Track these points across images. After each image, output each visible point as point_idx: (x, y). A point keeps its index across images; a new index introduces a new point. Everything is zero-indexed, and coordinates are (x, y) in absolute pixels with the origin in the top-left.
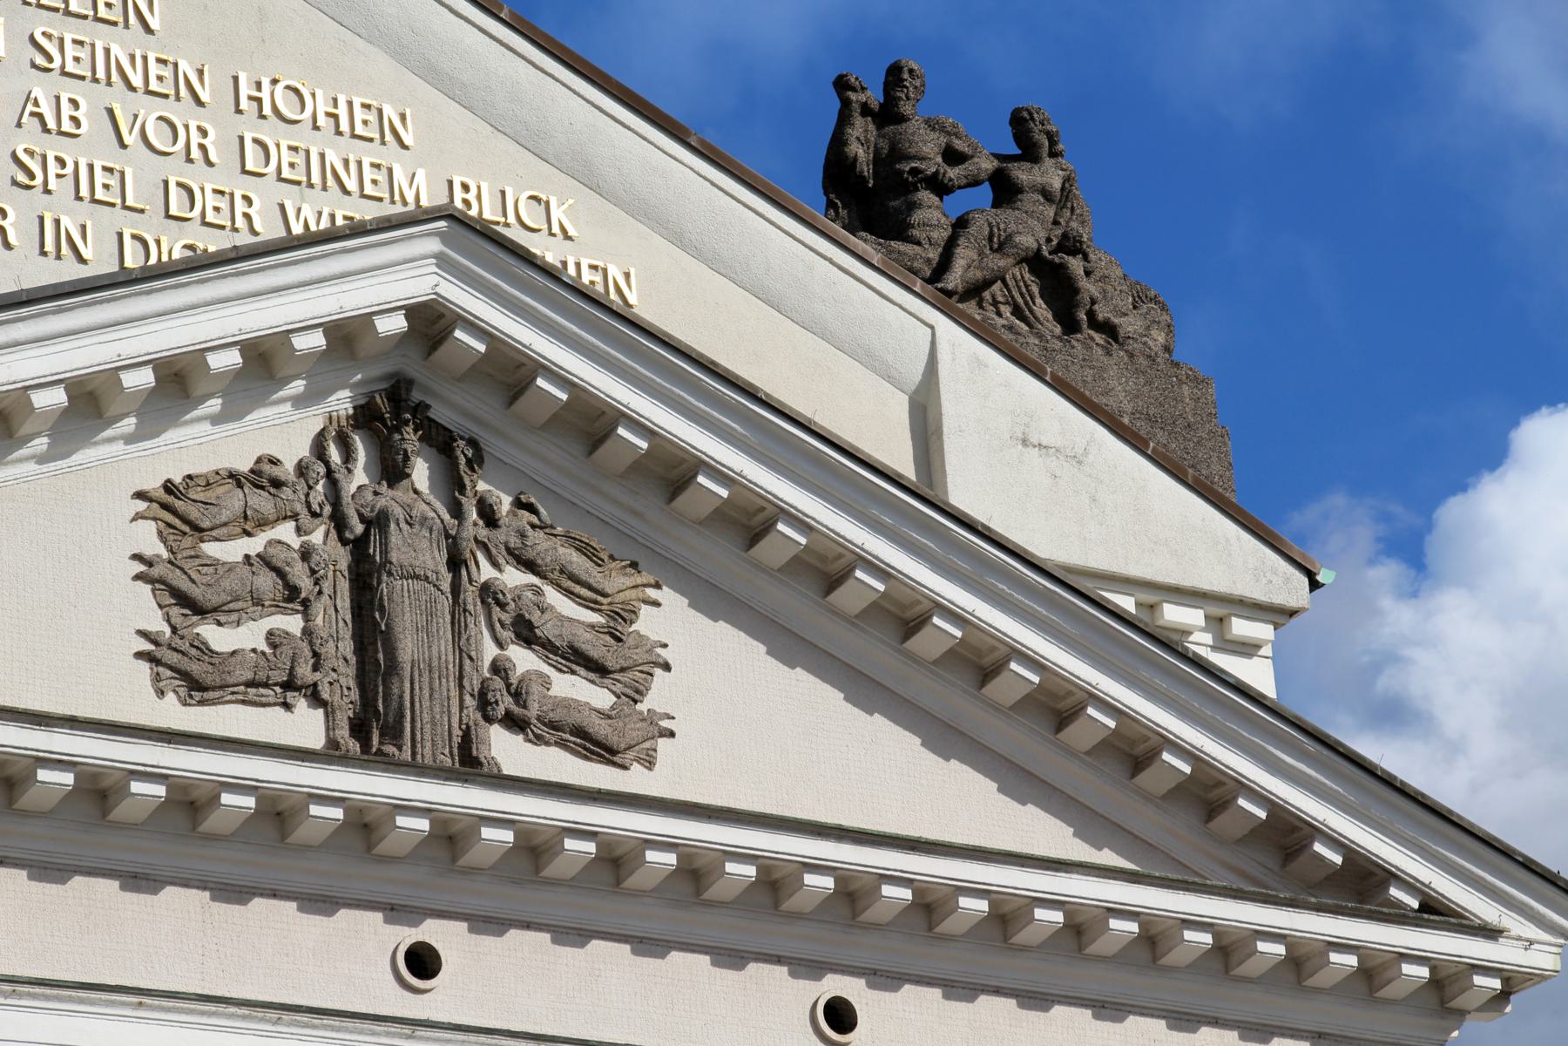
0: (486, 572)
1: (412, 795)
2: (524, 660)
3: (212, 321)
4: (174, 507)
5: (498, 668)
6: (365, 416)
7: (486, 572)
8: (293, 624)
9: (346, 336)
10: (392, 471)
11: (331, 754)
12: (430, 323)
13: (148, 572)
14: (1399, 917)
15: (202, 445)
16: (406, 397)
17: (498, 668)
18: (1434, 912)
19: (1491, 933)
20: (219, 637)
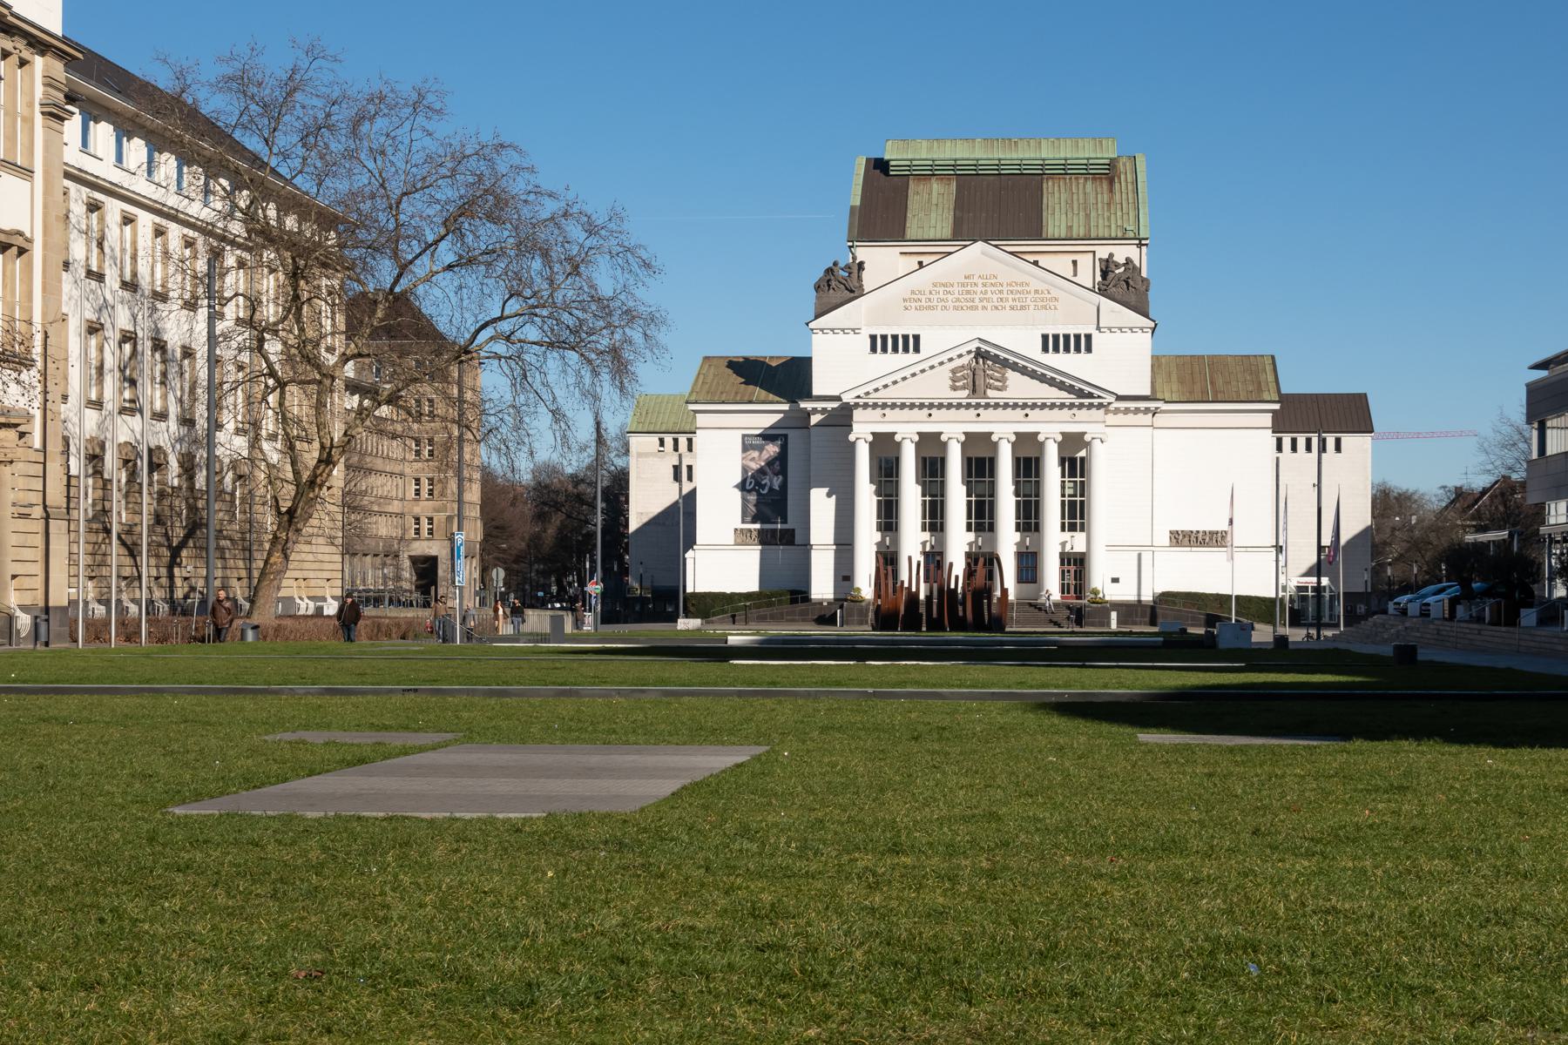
1: (973, 401)
3: (953, 354)
4: (953, 371)
9: (969, 352)
15: (958, 363)
16: (980, 354)
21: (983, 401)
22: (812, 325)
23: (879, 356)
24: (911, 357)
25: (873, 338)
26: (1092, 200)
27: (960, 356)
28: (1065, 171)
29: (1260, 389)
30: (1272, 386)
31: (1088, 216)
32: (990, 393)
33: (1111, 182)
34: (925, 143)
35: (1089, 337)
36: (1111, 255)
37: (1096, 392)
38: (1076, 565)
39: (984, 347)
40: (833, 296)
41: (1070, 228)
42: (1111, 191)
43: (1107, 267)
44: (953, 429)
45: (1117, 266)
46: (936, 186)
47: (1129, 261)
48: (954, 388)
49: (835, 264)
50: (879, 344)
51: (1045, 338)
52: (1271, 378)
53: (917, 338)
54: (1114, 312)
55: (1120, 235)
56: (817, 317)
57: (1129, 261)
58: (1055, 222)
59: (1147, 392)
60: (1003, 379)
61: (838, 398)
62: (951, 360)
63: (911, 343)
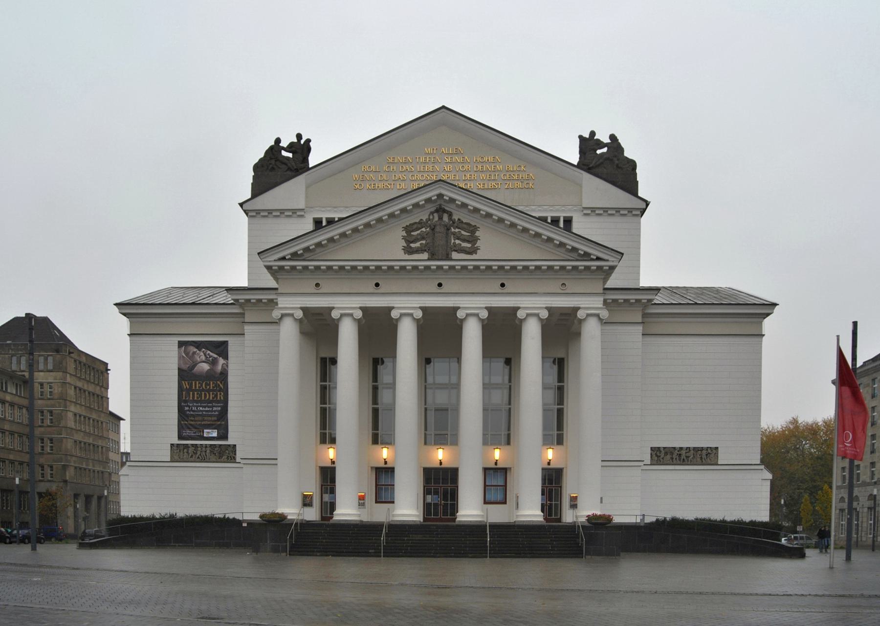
0: (453, 230)
2: (457, 242)
3: (407, 203)
5: (454, 243)
6: (437, 211)
7: (453, 230)
8: (424, 242)
9: (428, 201)
10: (441, 218)
11: (429, 259)
13: (404, 238)
14: (592, 260)
15: (414, 218)
17: (454, 243)
18: (598, 259)
19: (607, 260)
20: (413, 245)
21: (446, 264)
27: (416, 206)
32: (455, 255)
37: (595, 252)
39: (448, 194)
44: (407, 305)
60: (473, 240)
62: (404, 211)
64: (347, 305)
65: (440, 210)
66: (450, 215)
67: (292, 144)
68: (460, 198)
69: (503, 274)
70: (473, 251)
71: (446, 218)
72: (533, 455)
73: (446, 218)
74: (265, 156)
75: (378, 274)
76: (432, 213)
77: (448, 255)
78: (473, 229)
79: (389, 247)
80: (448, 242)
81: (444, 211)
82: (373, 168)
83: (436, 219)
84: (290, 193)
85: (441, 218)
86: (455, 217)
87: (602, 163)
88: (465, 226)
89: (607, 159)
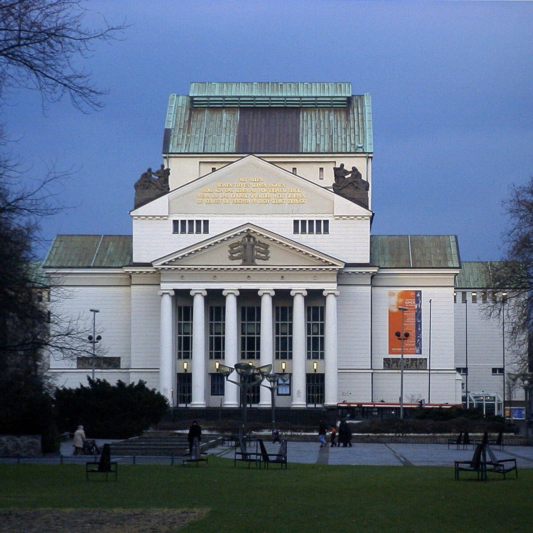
2: (258, 253)
4: (232, 246)
6: (247, 236)
8: (240, 253)
9: (243, 232)
10: (249, 240)
12: (249, 230)
13: (229, 251)
14: (330, 265)
15: (235, 240)
18: (333, 265)
19: (338, 266)
20: (234, 255)
22: (132, 214)
23: (179, 235)
24: (203, 237)
25: (175, 222)
26: (333, 126)
28: (316, 105)
29: (446, 260)
30: (455, 257)
31: (331, 137)
32: (257, 261)
33: (348, 114)
34: (217, 85)
35: (326, 222)
36: (342, 165)
37: (331, 261)
38: (316, 383)
39: (253, 229)
40: (148, 193)
41: (318, 145)
42: (347, 119)
43: (339, 172)
44: (231, 288)
45: (347, 173)
46: (225, 115)
47: (354, 169)
48: (232, 258)
49: (150, 170)
50: (179, 227)
51: (296, 222)
52: (454, 250)
53: (206, 222)
54: (344, 205)
55: (353, 151)
56: (137, 206)
57: (354, 169)
58: (308, 143)
59: (368, 261)
60: (267, 252)
61: (149, 265)
63: (203, 226)
64: (198, 288)
65: (249, 236)
66: (254, 239)
67: (158, 172)
68: (259, 232)
69: (282, 273)
70: (266, 259)
71: (252, 240)
72: (299, 366)
73: (252, 240)
74: (141, 178)
75: (214, 272)
76: (244, 238)
77: (253, 261)
78: (266, 246)
79: (221, 258)
80: (253, 253)
81: (251, 236)
82: (209, 190)
83: (247, 240)
84: (158, 206)
85: (249, 240)
86: (257, 240)
87: (347, 186)
88: (262, 245)
89: (350, 183)
